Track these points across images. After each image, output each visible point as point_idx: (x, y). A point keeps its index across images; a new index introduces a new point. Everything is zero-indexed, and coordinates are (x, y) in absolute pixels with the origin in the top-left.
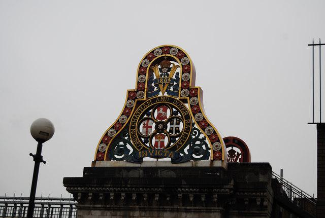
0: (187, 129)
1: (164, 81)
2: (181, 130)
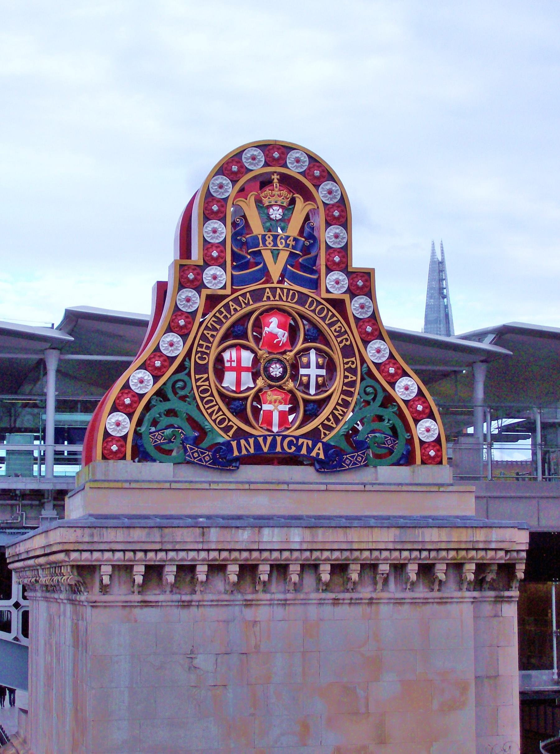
1: (275, 245)
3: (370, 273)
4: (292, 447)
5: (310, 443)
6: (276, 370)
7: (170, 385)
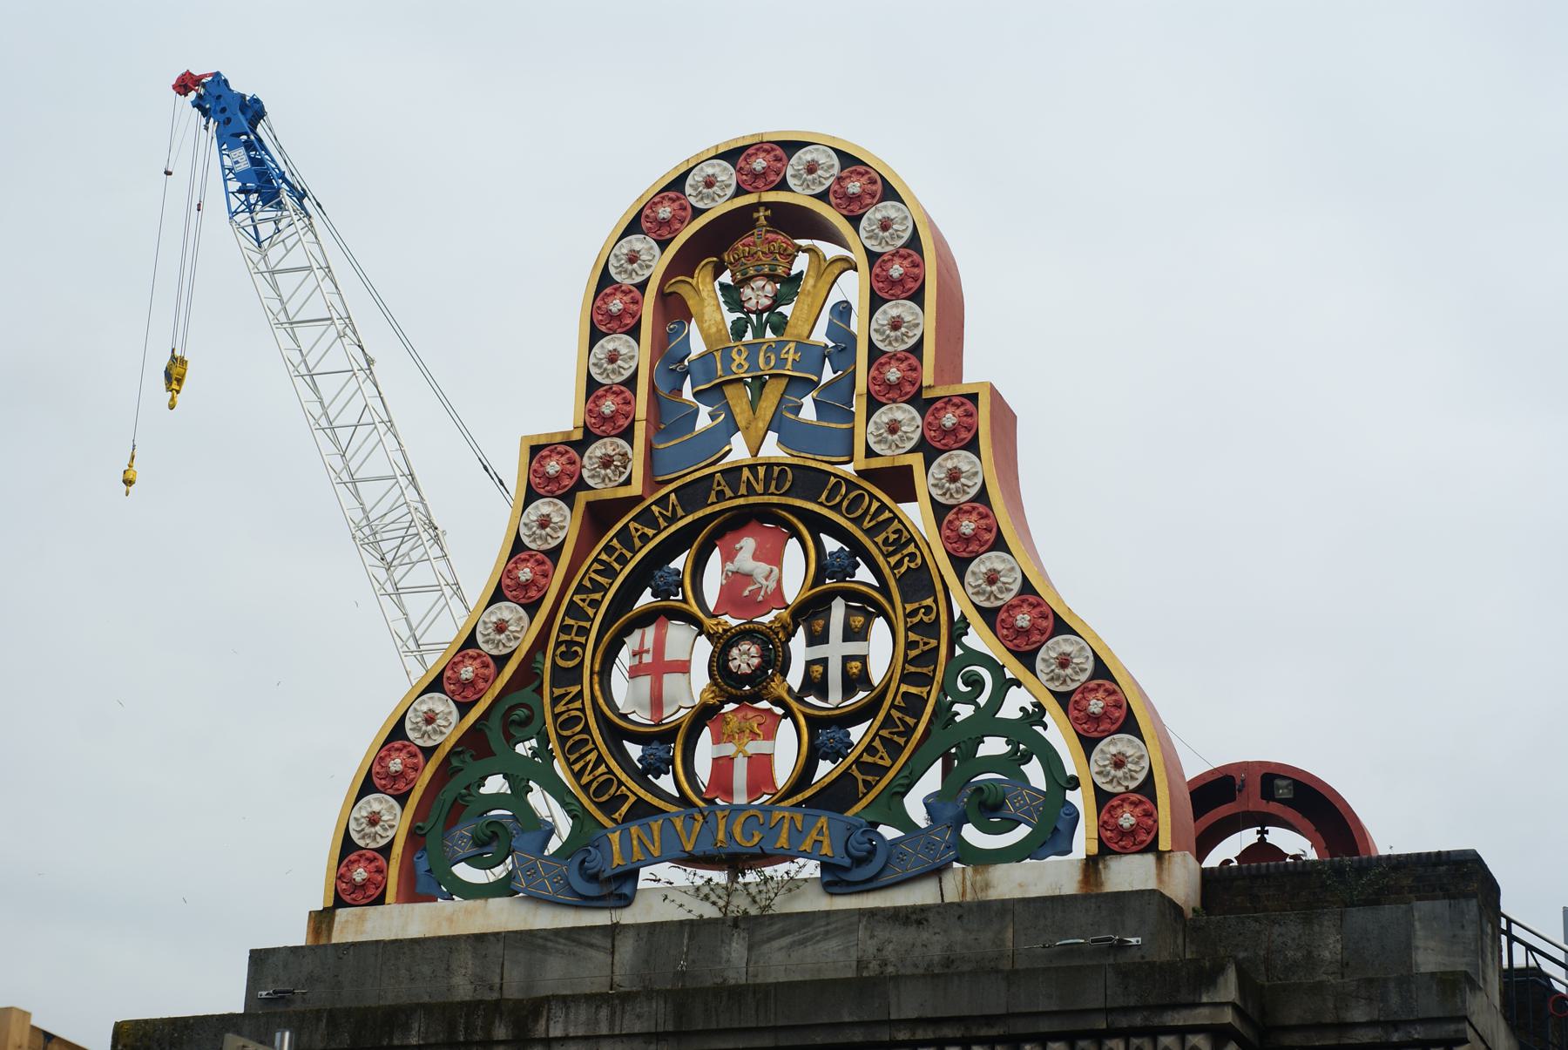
0: (913, 662)
1: (754, 366)
2: (877, 674)
3: (974, 398)
4: (756, 833)
5: (798, 817)
6: (745, 657)
7: (495, 723)
